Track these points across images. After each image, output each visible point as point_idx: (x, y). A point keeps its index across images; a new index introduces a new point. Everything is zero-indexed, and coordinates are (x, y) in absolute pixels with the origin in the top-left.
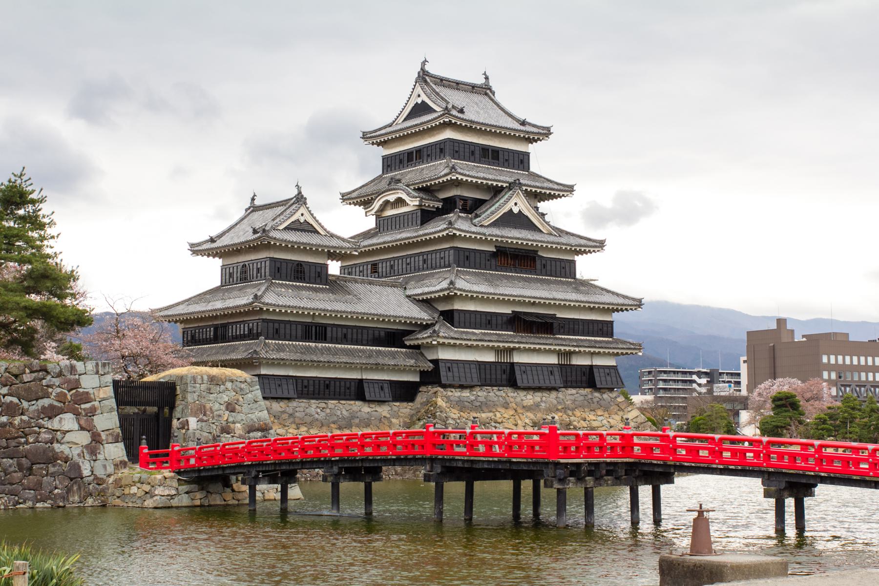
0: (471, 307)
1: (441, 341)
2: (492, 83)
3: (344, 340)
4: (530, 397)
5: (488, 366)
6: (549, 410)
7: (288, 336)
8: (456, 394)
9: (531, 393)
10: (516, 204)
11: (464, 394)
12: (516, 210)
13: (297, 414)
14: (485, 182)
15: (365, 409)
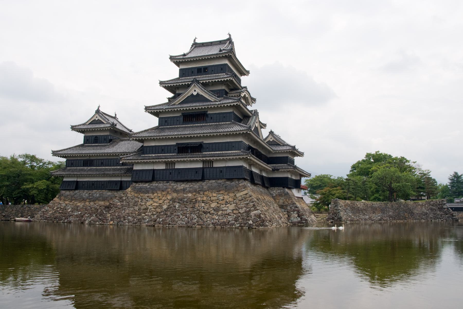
0: (153, 144)
1: (124, 161)
2: (232, 37)
3: (102, 164)
4: (183, 185)
5: (162, 172)
6: (190, 192)
7: (82, 165)
8: (141, 185)
9: (185, 183)
10: (195, 91)
11: (144, 185)
12: (195, 94)
13: (75, 196)
14: (178, 84)
15: (109, 193)
